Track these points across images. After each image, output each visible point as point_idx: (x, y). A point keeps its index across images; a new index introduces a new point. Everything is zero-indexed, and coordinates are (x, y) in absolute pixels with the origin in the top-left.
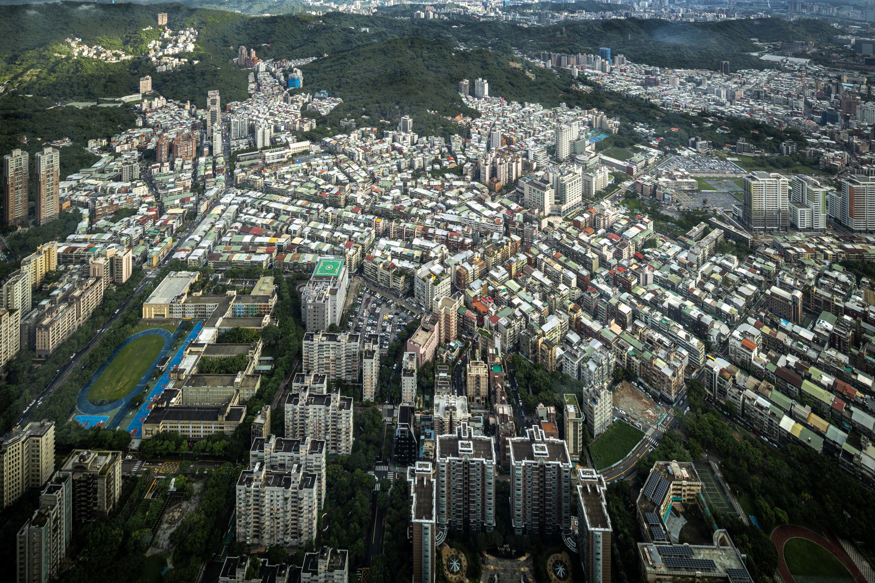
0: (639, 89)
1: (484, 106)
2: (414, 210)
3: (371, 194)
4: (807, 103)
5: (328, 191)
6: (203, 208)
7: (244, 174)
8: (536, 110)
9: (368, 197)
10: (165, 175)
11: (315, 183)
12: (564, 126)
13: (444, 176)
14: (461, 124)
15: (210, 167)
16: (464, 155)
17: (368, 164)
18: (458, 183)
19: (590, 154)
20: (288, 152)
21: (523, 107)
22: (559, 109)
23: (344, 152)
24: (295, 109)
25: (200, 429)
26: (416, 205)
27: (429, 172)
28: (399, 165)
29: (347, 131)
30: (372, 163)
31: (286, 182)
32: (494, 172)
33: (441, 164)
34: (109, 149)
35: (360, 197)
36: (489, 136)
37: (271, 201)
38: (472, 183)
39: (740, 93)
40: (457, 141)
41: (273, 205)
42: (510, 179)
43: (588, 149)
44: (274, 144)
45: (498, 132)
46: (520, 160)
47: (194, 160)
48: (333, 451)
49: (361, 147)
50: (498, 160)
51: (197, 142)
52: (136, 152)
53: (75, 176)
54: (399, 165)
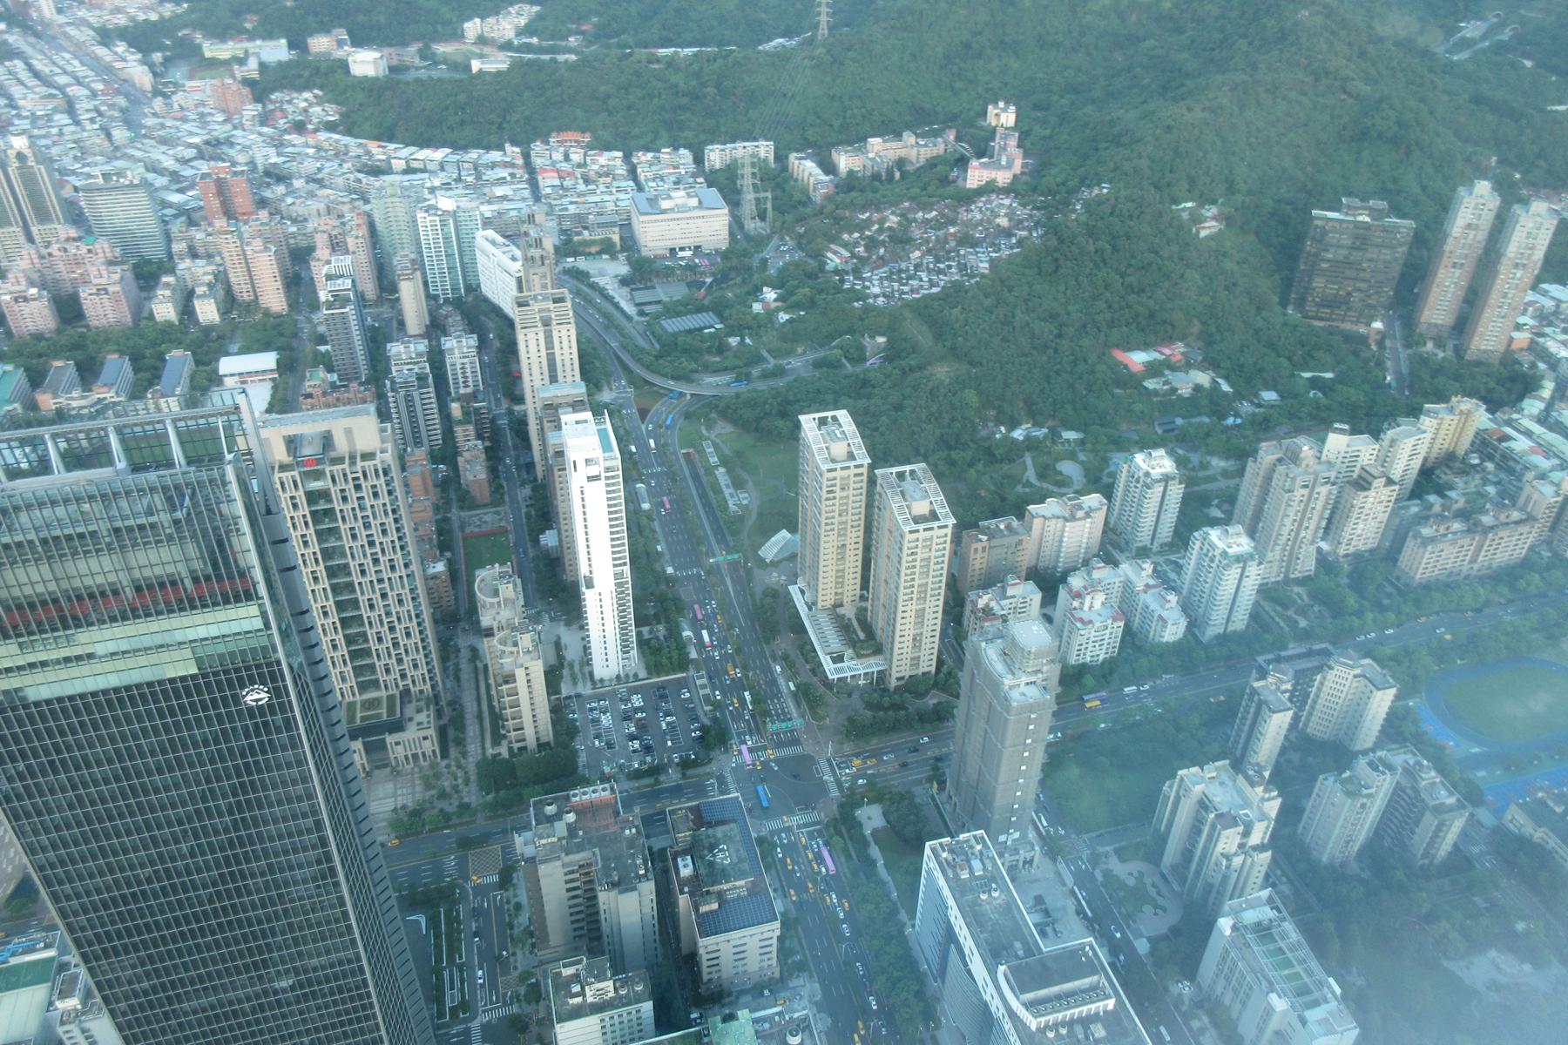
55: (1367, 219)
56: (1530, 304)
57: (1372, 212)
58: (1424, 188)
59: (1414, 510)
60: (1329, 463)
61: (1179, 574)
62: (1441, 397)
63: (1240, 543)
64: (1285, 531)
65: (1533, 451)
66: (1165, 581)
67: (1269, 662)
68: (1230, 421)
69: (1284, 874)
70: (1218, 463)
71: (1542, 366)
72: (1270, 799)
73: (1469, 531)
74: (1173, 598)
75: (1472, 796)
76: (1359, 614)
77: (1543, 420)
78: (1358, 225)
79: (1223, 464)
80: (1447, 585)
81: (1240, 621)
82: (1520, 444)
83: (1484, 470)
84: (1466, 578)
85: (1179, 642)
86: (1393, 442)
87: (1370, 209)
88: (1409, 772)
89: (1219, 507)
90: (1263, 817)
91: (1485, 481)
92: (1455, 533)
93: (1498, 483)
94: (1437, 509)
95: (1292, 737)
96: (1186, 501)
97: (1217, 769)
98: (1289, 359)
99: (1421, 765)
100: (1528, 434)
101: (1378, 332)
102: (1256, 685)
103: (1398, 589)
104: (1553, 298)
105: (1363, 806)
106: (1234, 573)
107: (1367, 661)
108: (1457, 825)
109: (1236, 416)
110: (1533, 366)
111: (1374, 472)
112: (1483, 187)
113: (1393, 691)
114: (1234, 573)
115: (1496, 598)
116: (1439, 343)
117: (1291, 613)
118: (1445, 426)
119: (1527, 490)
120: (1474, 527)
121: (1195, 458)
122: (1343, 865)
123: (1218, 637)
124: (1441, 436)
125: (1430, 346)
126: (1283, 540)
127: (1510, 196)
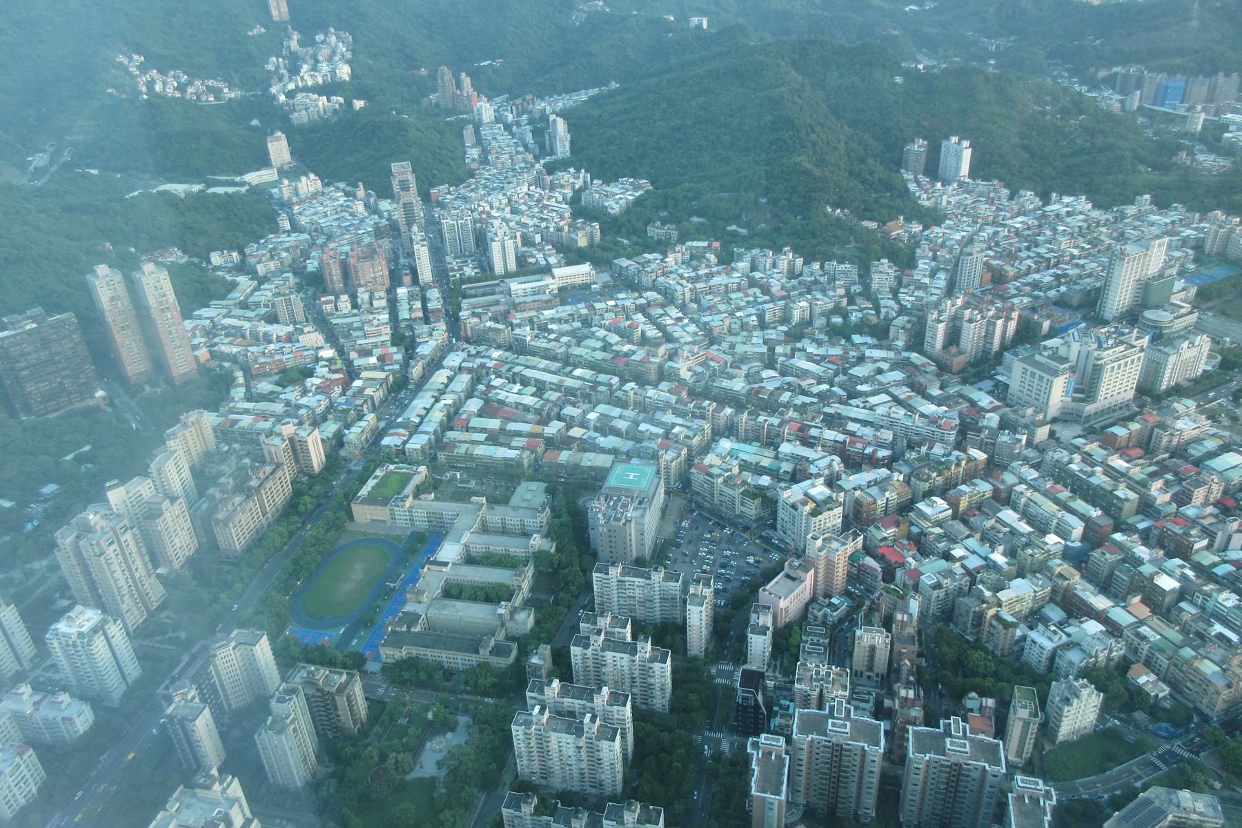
2: (786, 397)
3: (703, 364)
5: (626, 355)
6: (416, 371)
7: (476, 320)
9: (699, 369)
10: (345, 316)
11: (604, 340)
13: (848, 339)
15: (418, 304)
16: (898, 302)
17: (701, 309)
18: (877, 353)
20: (551, 284)
23: (654, 287)
24: (558, 203)
25: (458, 660)
26: (789, 387)
27: (820, 330)
28: (761, 317)
29: (662, 247)
30: (709, 308)
31: (552, 336)
32: (953, 337)
33: (845, 315)
34: (243, 268)
35: (684, 368)
36: (956, 265)
37: (527, 367)
38: (905, 354)
40: (883, 273)
41: (529, 373)
42: (986, 352)
43: (1175, 299)
44: (525, 268)
45: (978, 257)
46: (1015, 315)
47: (389, 291)
48: (644, 707)
49: (688, 279)
50: (967, 312)
51: (389, 261)
52: (290, 275)
53: (205, 312)
55: (34, 325)
56: (195, 327)
57: (34, 319)
58: (68, 285)
59: (205, 506)
60: (118, 515)
61: (57, 671)
62: (175, 420)
63: (87, 617)
64: (122, 583)
65: (256, 421)
66: (47, 688)
67: (167, 688)
68: (29, 527)
69: (282, 819)
70: (39, 565)
71: (227, 364)
72: (229, 785)
73: (248, 497)
74: (64, 698)
75: (356, 663)
76: (216, 600)
77: (249, 399)
78: (30, 333)
79: (44, 563)
80: (261, 539)
81: (133, 669)
82: (246, 421)
83: (235, 450)
84: (269, 525)
85: (95, 723)
86: (159, 471)
87: (30, 318)
88: (310, 682)
89: (62, 597)
90: (232, 801)
91: (240, 458)
92: (240, 505)
93: (248, 455)
94: (218, 495)
95: (226, 721)
96: (25, 616)
97: (177, 800)
98: (46, 453)
99: (312, 672)
100: (247, 412)
101: (104, 398)
102: (168, 711)
103: (232, 564)
104: (207, 318)
105: (295, 730)
106: (99, 643)
107: (235, 632)
108: (357, 689)
109: (31, 520)
110: (221, 367)
111: (158, 500)
112: (102, 269)
113: (265, 637)
114: (99, 641)
115: (294, 528)
116: (153, 384)
117: (170, 634)
118: (189, 438)
119: (264, 447)
120: (249, 493)
121: (17, 575)
122: (314, 775)
123: (125, 695)
124: (192, 446)
125: (147, 388)
126: (125, 590)
127: (127, 266)
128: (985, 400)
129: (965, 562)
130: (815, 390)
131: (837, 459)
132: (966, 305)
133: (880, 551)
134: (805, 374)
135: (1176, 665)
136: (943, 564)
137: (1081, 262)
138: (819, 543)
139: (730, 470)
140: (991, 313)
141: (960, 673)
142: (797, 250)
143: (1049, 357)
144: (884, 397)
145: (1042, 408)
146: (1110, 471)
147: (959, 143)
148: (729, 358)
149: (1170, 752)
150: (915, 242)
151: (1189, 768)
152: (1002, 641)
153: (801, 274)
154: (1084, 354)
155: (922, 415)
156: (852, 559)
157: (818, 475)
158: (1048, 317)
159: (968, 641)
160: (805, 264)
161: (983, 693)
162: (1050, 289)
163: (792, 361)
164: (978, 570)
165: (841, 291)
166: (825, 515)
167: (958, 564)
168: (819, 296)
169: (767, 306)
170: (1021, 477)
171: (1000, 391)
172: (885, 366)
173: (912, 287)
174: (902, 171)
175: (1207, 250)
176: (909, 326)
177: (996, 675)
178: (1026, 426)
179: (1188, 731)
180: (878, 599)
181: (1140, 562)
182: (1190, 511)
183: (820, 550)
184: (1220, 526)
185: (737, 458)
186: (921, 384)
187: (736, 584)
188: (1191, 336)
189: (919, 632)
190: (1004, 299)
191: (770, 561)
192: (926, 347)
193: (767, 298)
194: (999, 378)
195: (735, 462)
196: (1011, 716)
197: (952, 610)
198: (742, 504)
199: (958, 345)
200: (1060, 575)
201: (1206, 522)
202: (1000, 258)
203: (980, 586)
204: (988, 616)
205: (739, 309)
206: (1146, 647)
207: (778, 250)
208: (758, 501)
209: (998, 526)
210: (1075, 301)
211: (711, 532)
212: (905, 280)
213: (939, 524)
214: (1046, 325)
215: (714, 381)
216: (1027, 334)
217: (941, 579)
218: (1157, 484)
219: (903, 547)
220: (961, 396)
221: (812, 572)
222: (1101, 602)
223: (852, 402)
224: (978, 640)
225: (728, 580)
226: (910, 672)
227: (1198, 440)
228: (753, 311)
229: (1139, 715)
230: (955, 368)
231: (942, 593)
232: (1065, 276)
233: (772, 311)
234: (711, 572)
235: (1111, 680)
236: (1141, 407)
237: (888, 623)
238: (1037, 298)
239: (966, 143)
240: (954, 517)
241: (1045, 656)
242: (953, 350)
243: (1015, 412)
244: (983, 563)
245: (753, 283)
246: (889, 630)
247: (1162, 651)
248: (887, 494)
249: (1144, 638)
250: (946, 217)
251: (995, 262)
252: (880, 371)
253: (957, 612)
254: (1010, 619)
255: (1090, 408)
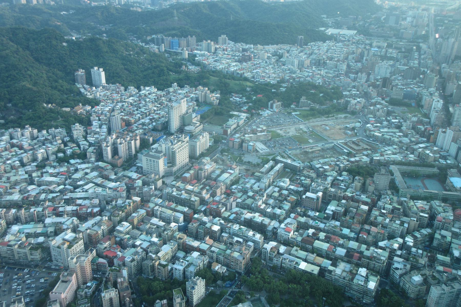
0: (236, 66)
1: (102, 94)
4: (348, 66)
8: (150, 91)
12: (174, 104)
13: (68, 162)
14: (81, 114)
16: (88, 141)
18: (83, 166)
19: (196, 124)
21: (140, 90)
22: (171, 90)
26: (44, 191)
28: (21, 161)
32: (115, 152)
33: (64, 152)
36: (109, 121)
38: (96, 164)
39: (307, 62)
40: (78, 130)
42: (130, 155)
43: (194, 121)
45: (118, 117)
46: (138, 138)
54: (21, 161)
128: (134, 175)
129: (142, 246)
130: (57, 189)
131: (75, 219)
132: (117, 137)
133: (104, 254)
134: (50, 183)
135: (226, 258)
136: (133, 250)
137: (158, 112)
138: (75, 260)
139: (21, 240)
140: (128, 139)
141: (151, 294)
142: (32, 126)
143: (155, 152)
144: (91, 185)
145: (157, 173)
146: (188, 192)
147: (98, 70)
148: (8, 185)
149: (232, 292)
150: (89, 114)
151: (239, 295)
152: (164, 273)
153: (38, 137)
154: (167, 148)
155: (110, 188)
156: (93, 262)
157: (68, 229)
158: (151, 136)
159: (151, 279)
160: (39, 132)
161: (161, 299)
162: (149, 124)
163: (42, 179)
164: (148, 248)
165: (60, 141)
166: (75, 246)
167: (139, 248)
168: (49, 145)
169: (23, 155)
170: (156, 203)
171: (140, 170)
172: (88, 171)
173: (93, 134)
174: (76, 84)
175: (200, 101)
176: (95, 151)
177: (165, 289)
178: (153, 182)
179: (236, 281)
180: (108, 276)
181: (205, 223)
182: (217, 199)
183: (76, 263)
184: (228, 201)
185: (23, 233)
186: (106, 175)
187: (37, 295)
188: (202, 134)
189: (130, 283)
190: (132, 132)
191: (52, 277)
192: (105, 159)
193: (22, 151)
194: (138, 165)
195: (23, 235)
196: (174, 303)
197: (141, 268)
198: (31, 254)
199: (118, 155)
200: (180, 238)
201: (223, 201)
202: (127, 115)
203: (150, 254)
204: (156, 265)
205: (8, 159)
206: (215, 255)
207: (23, 128)
208: (39, 251)
209: (152, 226)
210: (160, 128)
211: (17, 274)
212: (89, 131)
213: (128, 233)
214: (151, 139)
215: (2, 198)
216: (145, 145)
217: (133, 256)
218: (204, 191)
219: (115, 248)
220: (124, 176)
221: (74, 275)
222: (196, 244)
223: (77, 190)
224: (155, 277)
225: (32, 295)
226: (130, 303)
227: (213, 172)
228: (16, 159)
229: (219, 282)
230: (119, 166)
231: (135, 263)
232: (154, 118)
233: (26, 157)
234: (21, 295)
235: (206, 273)
236: (192, 164)
237: (115, 285)
238: (145, 129)
239: (101, 70)
240: (133, 228)
241: (181, 273)
242: (116, 157)
243: (147, 177)
244: (149, 243)
245: (13, 146)
246: (116, 288)
247: (220, 254)
248: (102, 227)
249: (213, 252)
250: (100, 102)
251: (125, 118)
252: (86, 174)
253: (144, 268)
254: (165, 263)
255: (175, 169)
